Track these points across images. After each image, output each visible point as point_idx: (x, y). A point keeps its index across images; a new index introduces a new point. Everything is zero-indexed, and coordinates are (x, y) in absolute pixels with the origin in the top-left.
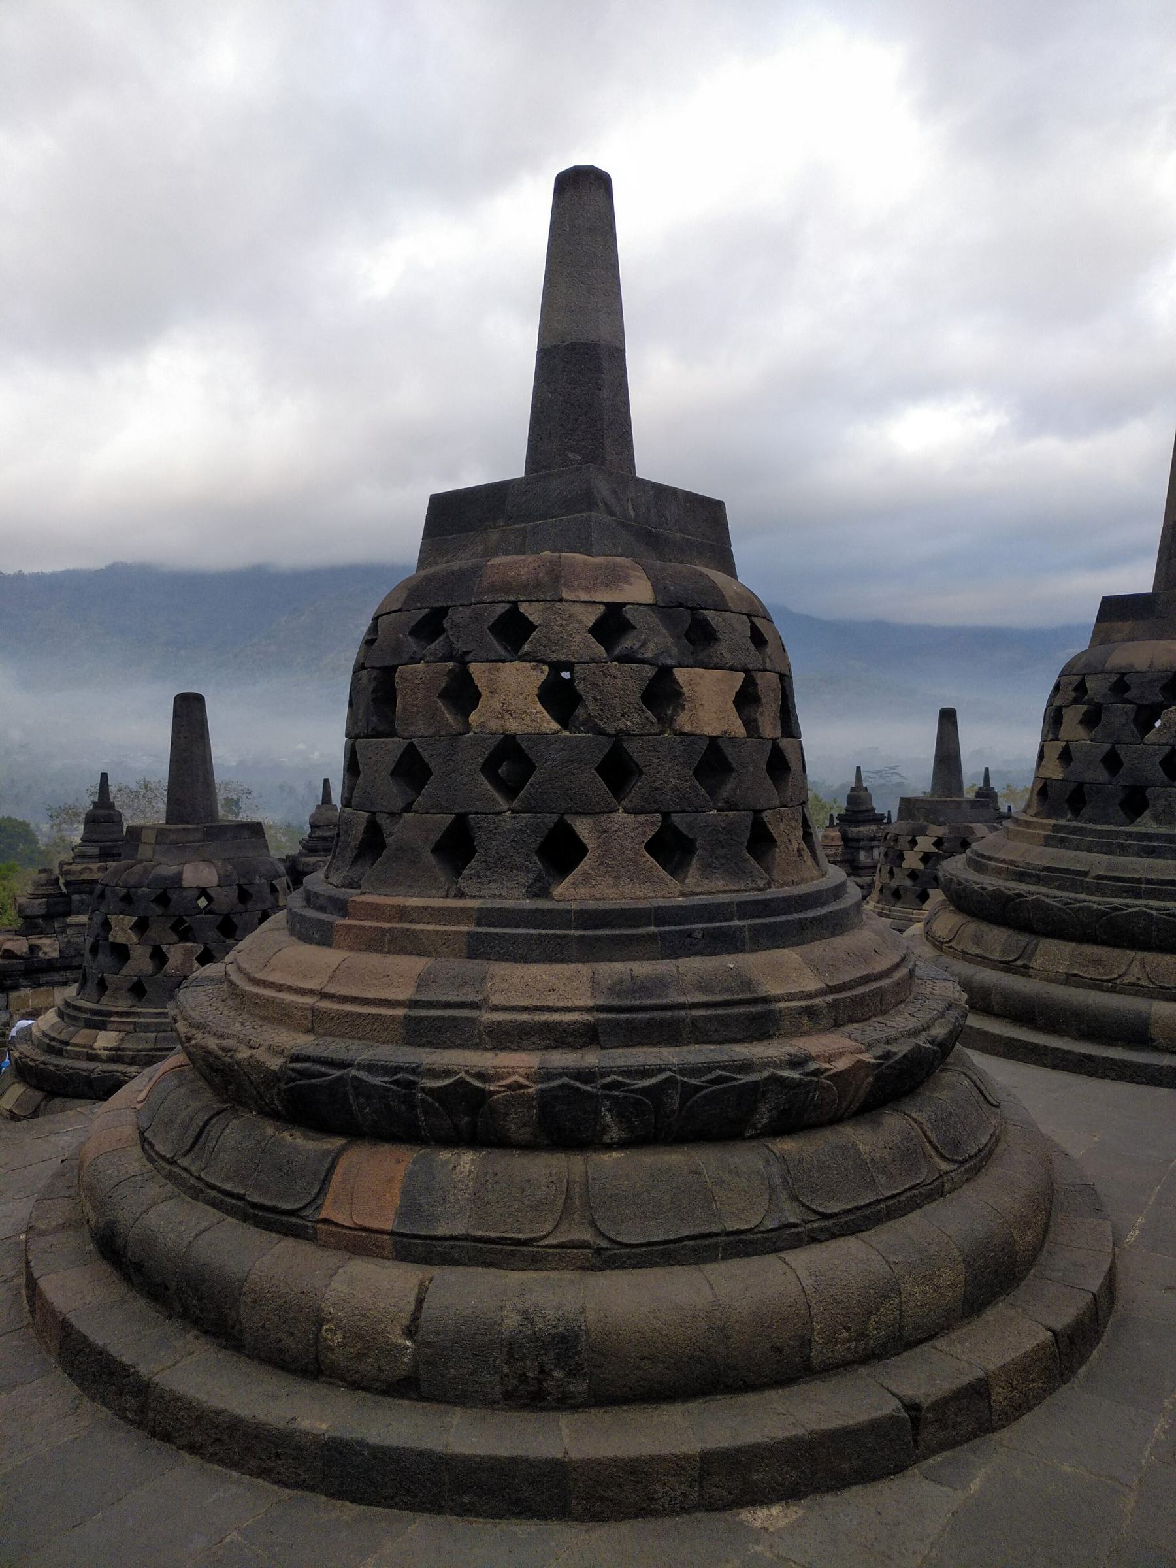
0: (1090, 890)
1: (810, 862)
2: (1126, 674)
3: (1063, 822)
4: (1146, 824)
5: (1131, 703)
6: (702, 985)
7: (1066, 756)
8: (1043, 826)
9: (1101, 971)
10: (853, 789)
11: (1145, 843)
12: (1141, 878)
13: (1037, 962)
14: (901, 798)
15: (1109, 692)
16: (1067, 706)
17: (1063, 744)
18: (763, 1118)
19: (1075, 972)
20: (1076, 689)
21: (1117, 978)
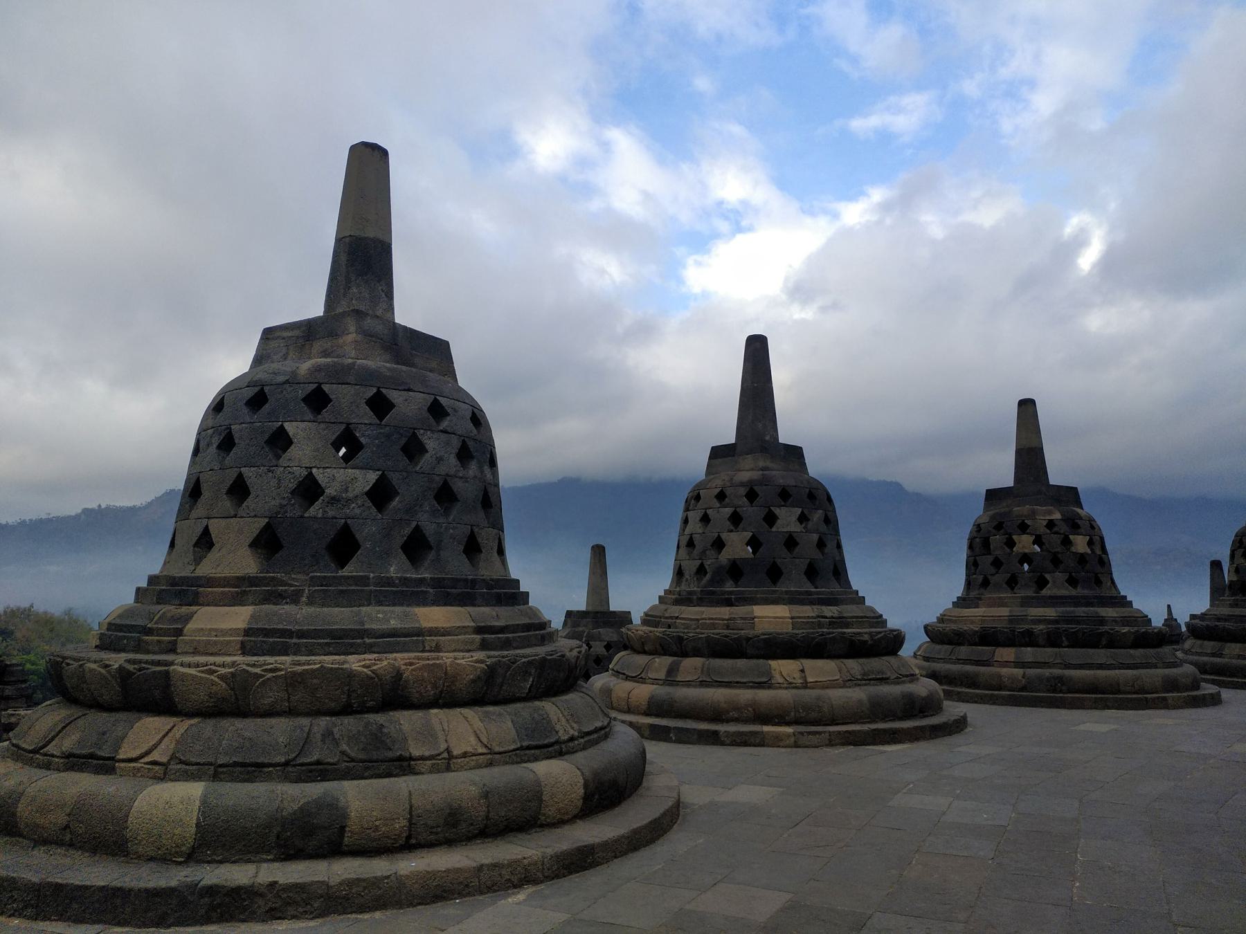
1: (1114, 589)
6: (1084, 612)
7: (1237, 571)
8: (1229, 600)
10: (1166, 620)
13: (1226, 651)
14: (1191, 615)
18: (1104, 642)
20: (1239, 543)
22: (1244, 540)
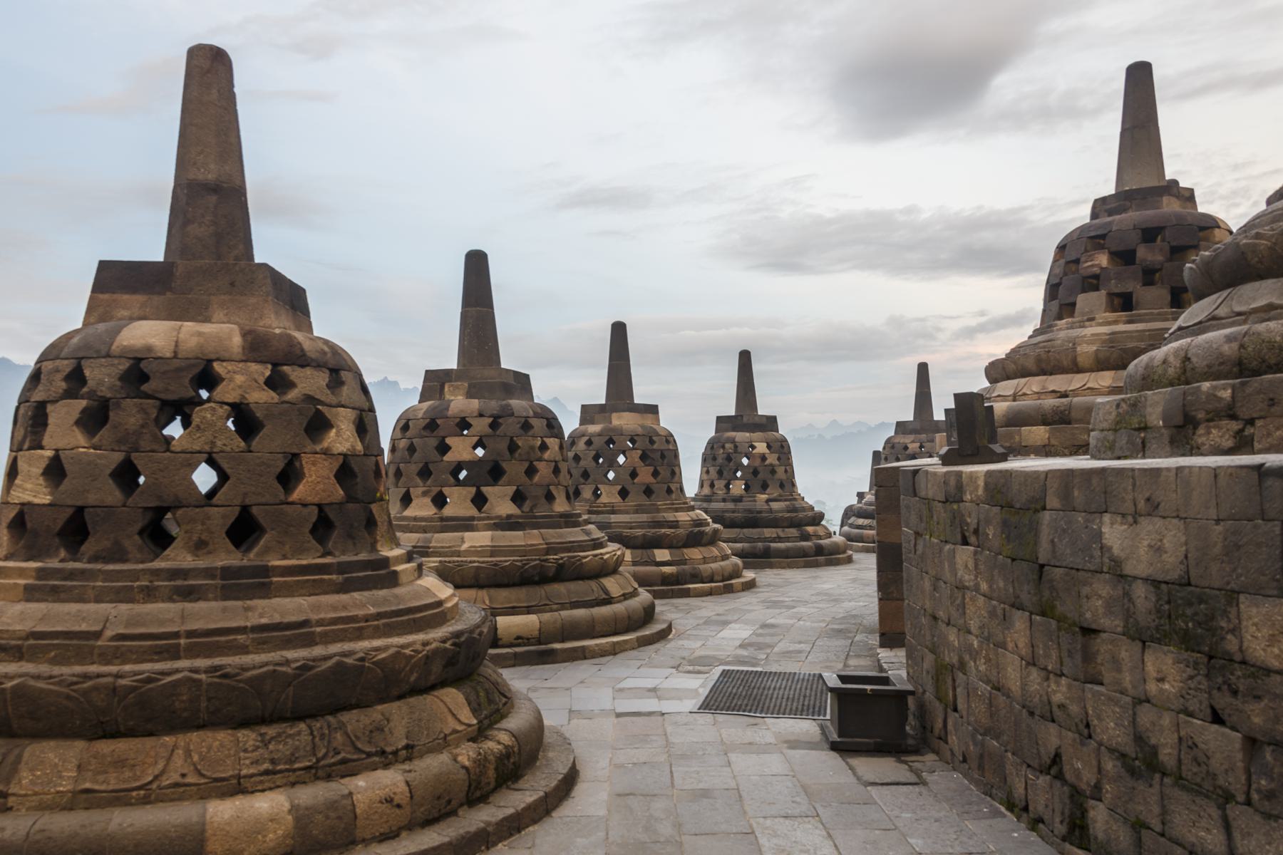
0: (105, 657)
2: (143, 359)
3: (54, 563)
4: (178, 557)
5: (148, 396)
7: (55, 471)
8: (21, 573)
9: (128, 774)
11: (179, 583)
12: (178, 632)
15: (118, 383)
16: (54, 402)
17: (49, 453)
19: (88, 785)
20: (68, 378)
21: (151, 782)
22: (87, 373)
